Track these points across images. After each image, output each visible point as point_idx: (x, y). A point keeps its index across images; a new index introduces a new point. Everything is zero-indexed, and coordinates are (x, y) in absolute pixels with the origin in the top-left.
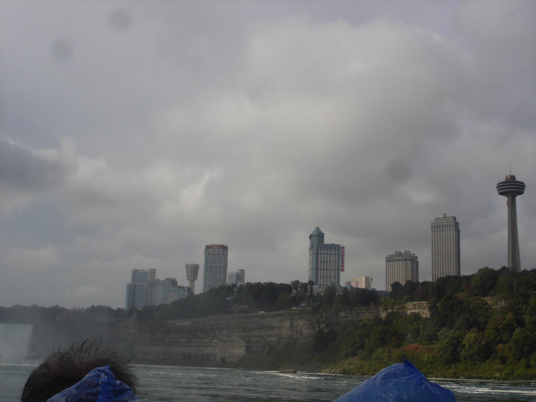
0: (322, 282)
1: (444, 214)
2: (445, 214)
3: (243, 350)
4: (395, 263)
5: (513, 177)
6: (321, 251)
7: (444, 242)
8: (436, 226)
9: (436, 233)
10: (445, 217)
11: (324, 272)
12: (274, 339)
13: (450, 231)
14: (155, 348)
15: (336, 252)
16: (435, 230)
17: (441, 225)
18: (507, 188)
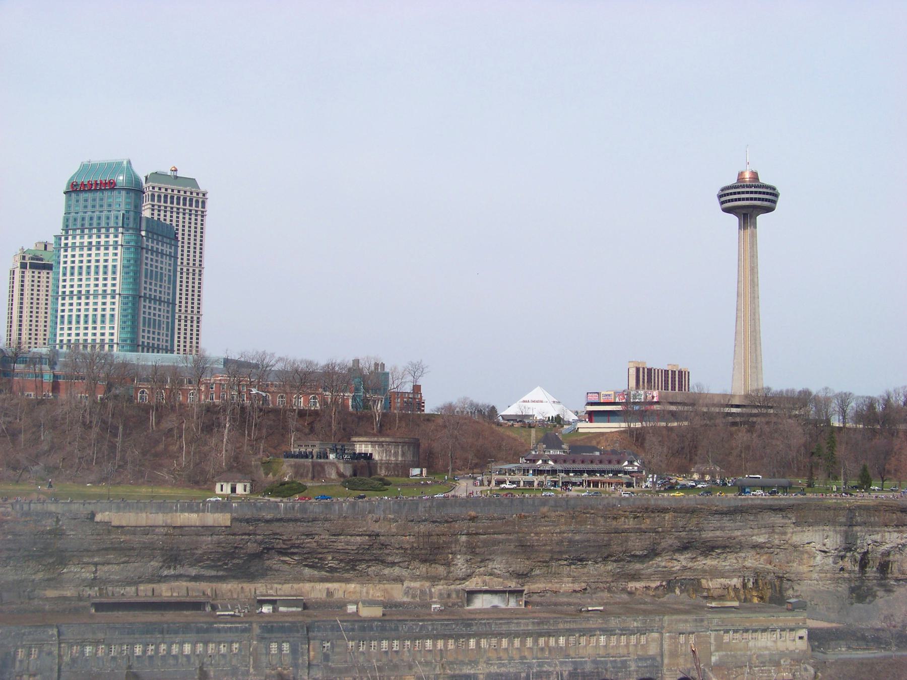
0: (107, 334)
1: (173, 169)
2: (176, 170)
3: (801, 638)
4: (39, 273)
5: (755, 176)
6: (147, 241)
7: (192, 242)
8: (163, 195)
9: (187, 216)
10: (176, 177)
11: (104, 304)
12: (736, 582)
13: (165, 212)
14: (187, 648)
15: (84, 239)
16: (159, 206)
17: (188, 199)
18: (759, 199)
